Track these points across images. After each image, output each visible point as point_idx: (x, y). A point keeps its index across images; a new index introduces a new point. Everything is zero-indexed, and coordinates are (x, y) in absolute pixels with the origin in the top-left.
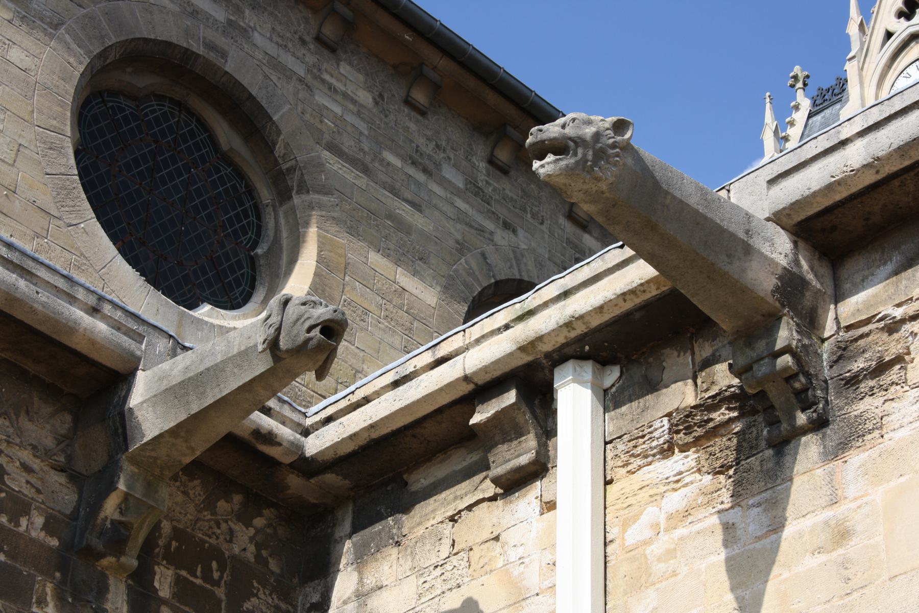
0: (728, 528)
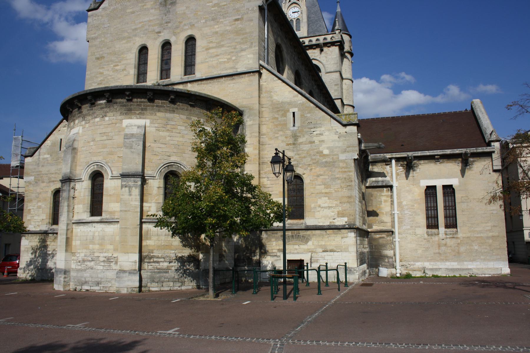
0: (405, 174)
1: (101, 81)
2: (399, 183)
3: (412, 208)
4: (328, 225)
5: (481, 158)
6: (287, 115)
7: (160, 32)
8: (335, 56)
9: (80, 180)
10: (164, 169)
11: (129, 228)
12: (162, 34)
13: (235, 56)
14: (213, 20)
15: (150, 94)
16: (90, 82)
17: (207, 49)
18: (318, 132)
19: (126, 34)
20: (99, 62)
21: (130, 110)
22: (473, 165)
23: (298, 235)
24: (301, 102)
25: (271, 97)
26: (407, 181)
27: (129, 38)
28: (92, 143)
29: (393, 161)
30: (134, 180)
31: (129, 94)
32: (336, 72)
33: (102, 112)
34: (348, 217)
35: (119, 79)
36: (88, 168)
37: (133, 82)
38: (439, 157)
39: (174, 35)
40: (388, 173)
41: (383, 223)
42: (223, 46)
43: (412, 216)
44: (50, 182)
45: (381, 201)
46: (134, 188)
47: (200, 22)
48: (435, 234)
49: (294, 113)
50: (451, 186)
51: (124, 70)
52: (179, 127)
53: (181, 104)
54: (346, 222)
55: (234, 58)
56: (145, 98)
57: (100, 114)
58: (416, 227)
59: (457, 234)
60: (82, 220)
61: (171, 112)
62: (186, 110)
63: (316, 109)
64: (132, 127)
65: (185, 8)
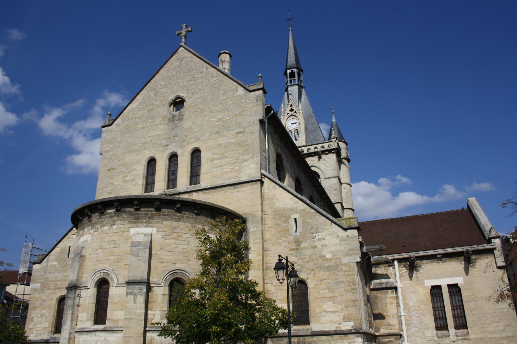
0: (409, 275)
1: (111, 190)
2: (403, 284)
3: (419, 310)
4: (334, 330)
5: (483, 255)
6: (289, 221)
7: (167, 145)
8: (333, 163)
9: (86, 288)
10: (169, 276)
11: (132, 337)
12: (169, 147)
13: (238, 166)
14: (217, 133)
15: (157, 204)
16: (101, 192)
17: (212, 160)
18: (320, 237)
19: (136, 148)
20: (110, 173)
21: (138, 219)
22: (476, 262)
23: (304, 342)
24: (302, 208)
25: (273, 204)
26: (411, 281)
27: (139, 150)
28: (99, 251)
29: (396, 263)
30: (139, 288)
31: (137, 203)
32: (335, 177)
33: (111, 220)
34: (354, 321)
35: (128, 189)
36: (94, 276)
37: (141, 191)
38: (441, 256)
39: (181, 148)
40: (391, 274)
41: (390, 326)
42: (226, 157)
43: (420, 318)
44: (56, 289)
45: (387, 304)
46: (139, 296)
47: (205, 136)
48: (445, 336)
49: (295, 219)
50: (456, 285)
51: (134, 180)
52: (184, 235)
53: (186, 213)
54: (352, 327)
55: (237, 168)
56: (153, 207)
57: (108, 223)
58: (424, 329)
59: (469, 335)
60: (86, 328)
61: (177, 220)
62: (191, 219)
63: (316, 214)
64: (139, 235)
65: (191, 123)
